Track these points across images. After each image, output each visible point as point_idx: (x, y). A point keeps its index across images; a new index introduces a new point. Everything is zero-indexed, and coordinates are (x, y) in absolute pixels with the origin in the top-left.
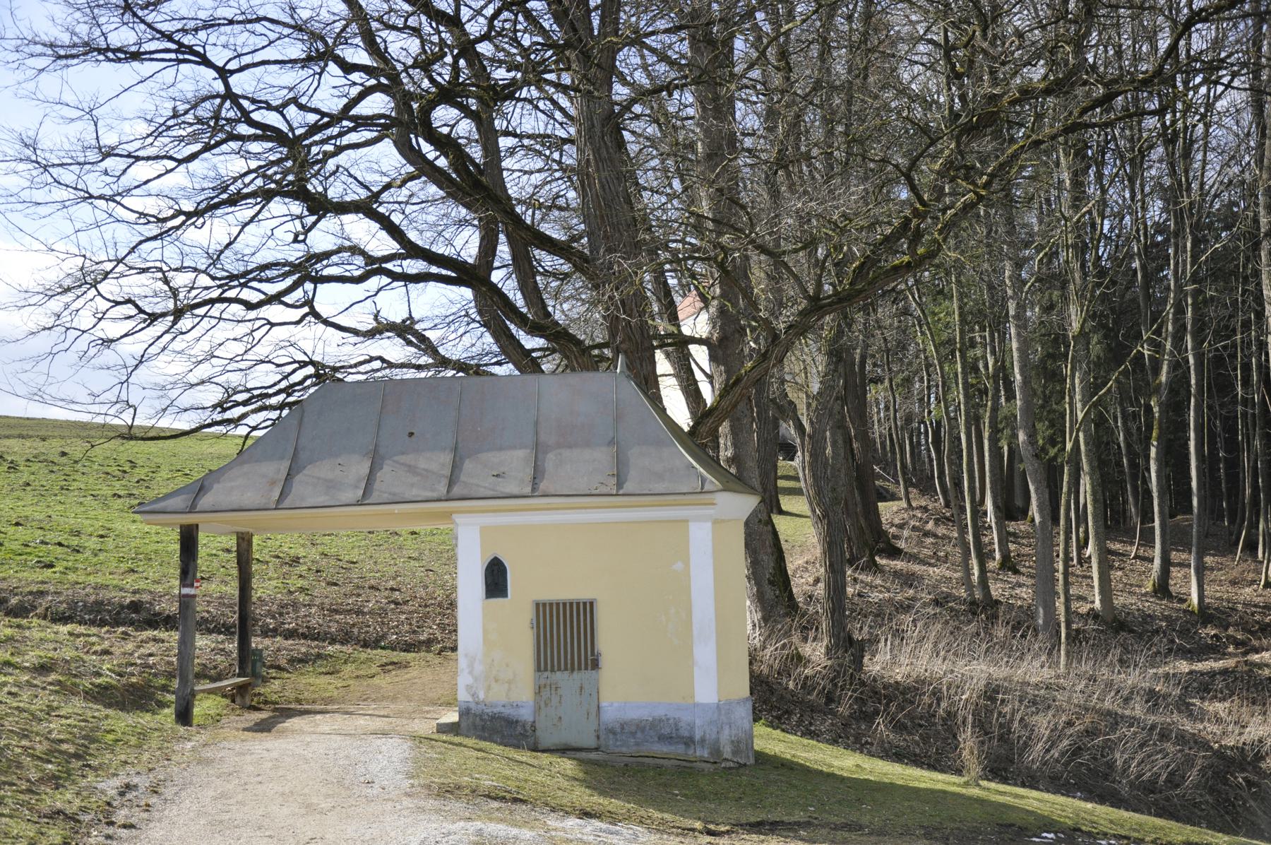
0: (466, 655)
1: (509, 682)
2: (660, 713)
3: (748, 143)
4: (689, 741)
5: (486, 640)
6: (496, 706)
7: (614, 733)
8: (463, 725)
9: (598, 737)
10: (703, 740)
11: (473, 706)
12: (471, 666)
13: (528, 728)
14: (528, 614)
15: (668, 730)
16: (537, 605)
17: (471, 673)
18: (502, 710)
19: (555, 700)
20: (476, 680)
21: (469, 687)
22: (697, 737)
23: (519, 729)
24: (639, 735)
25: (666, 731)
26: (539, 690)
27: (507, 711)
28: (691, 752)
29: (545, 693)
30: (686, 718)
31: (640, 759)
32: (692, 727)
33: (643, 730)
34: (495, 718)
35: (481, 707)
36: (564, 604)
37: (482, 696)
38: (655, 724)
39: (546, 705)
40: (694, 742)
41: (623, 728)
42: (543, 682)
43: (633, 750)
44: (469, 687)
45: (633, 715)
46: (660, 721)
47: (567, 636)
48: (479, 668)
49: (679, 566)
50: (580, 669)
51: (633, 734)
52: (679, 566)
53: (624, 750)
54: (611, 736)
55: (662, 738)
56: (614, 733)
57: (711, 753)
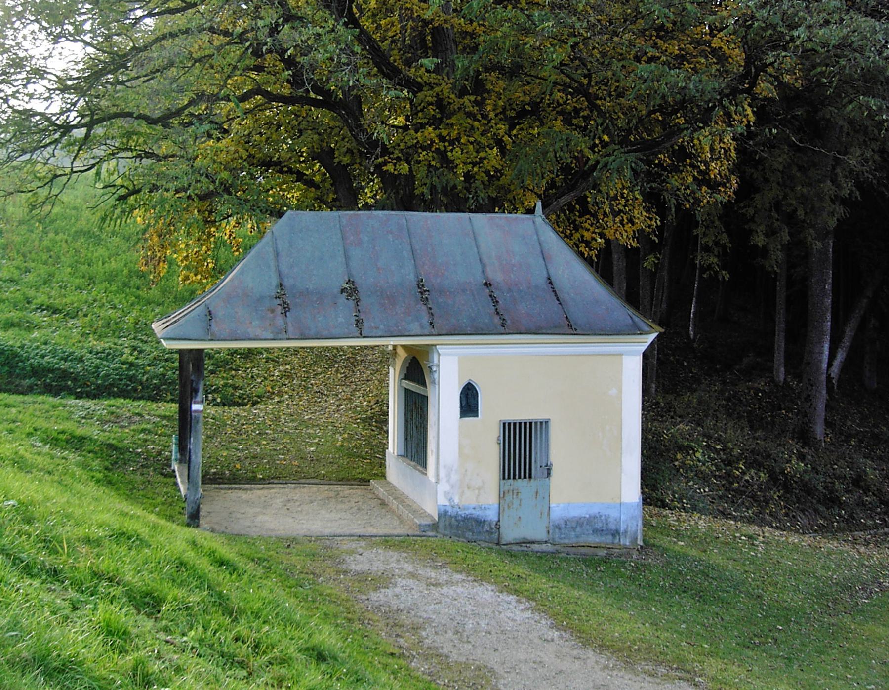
0: (445, 467)
1: (479, 489)
2: (594, 511)
3: (538, 44)
4: (616, 533)
5: (461, 454)
6: (468, 509)
7: (560, 529)
8: (441, 525)
9: (548, 532)
10: (626, 532)
11: (450, 509)
12: (449, 475)
13: (493, 526)
14: (494, 433)
15: (600, 525)
16: (504, 424)
17: (448, 481)
18: (473, 512)
19: (516, 502)
20: (452, 487)
21: (446, 494)
22: (622, 529)
23: (486, 528)
24: (578, 529)
25: (599, 525)
26: (502, 496)
27: (477, 513)
28: (617, 541)
29: (508, 498)
30: (613, 514)
31: (582, 550)
32: (618, 520)
33: (581, 525)
34: (467, 519)
35: (456, 509)
36: (515, 424)
37: (456, 501)
38: (590, 520)
39: (509, 507)
40: (619, 534)
41: (566, 524)
42: (506, 488)
43: (573, 541)
44: (446, 494)
45: (575, 513)
46: (595, 517)
47: (522, 449)
48: (455, 477)
49: (614, 392)
50: (514, 478)
51: (574, 529)
52: (614, 392)
53: (567, 541)
54: (557, 531)
55: (595, 531)
56: (560, 529)
57: (631, 542)
